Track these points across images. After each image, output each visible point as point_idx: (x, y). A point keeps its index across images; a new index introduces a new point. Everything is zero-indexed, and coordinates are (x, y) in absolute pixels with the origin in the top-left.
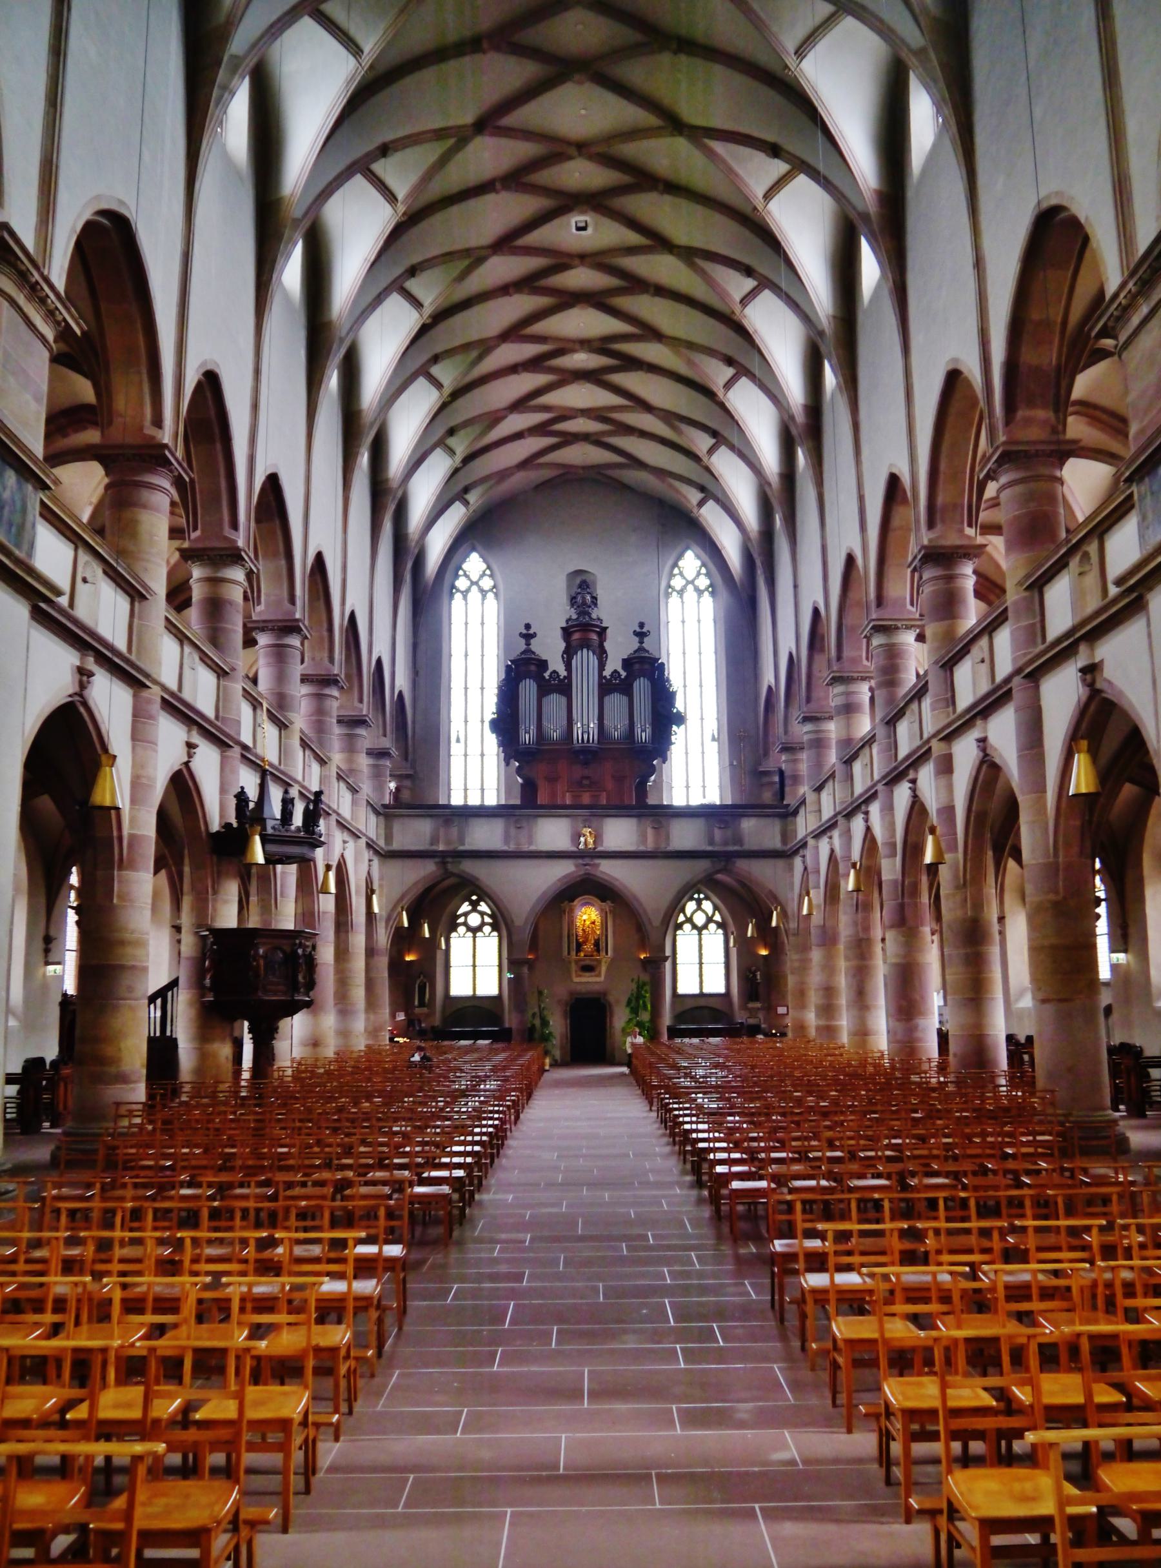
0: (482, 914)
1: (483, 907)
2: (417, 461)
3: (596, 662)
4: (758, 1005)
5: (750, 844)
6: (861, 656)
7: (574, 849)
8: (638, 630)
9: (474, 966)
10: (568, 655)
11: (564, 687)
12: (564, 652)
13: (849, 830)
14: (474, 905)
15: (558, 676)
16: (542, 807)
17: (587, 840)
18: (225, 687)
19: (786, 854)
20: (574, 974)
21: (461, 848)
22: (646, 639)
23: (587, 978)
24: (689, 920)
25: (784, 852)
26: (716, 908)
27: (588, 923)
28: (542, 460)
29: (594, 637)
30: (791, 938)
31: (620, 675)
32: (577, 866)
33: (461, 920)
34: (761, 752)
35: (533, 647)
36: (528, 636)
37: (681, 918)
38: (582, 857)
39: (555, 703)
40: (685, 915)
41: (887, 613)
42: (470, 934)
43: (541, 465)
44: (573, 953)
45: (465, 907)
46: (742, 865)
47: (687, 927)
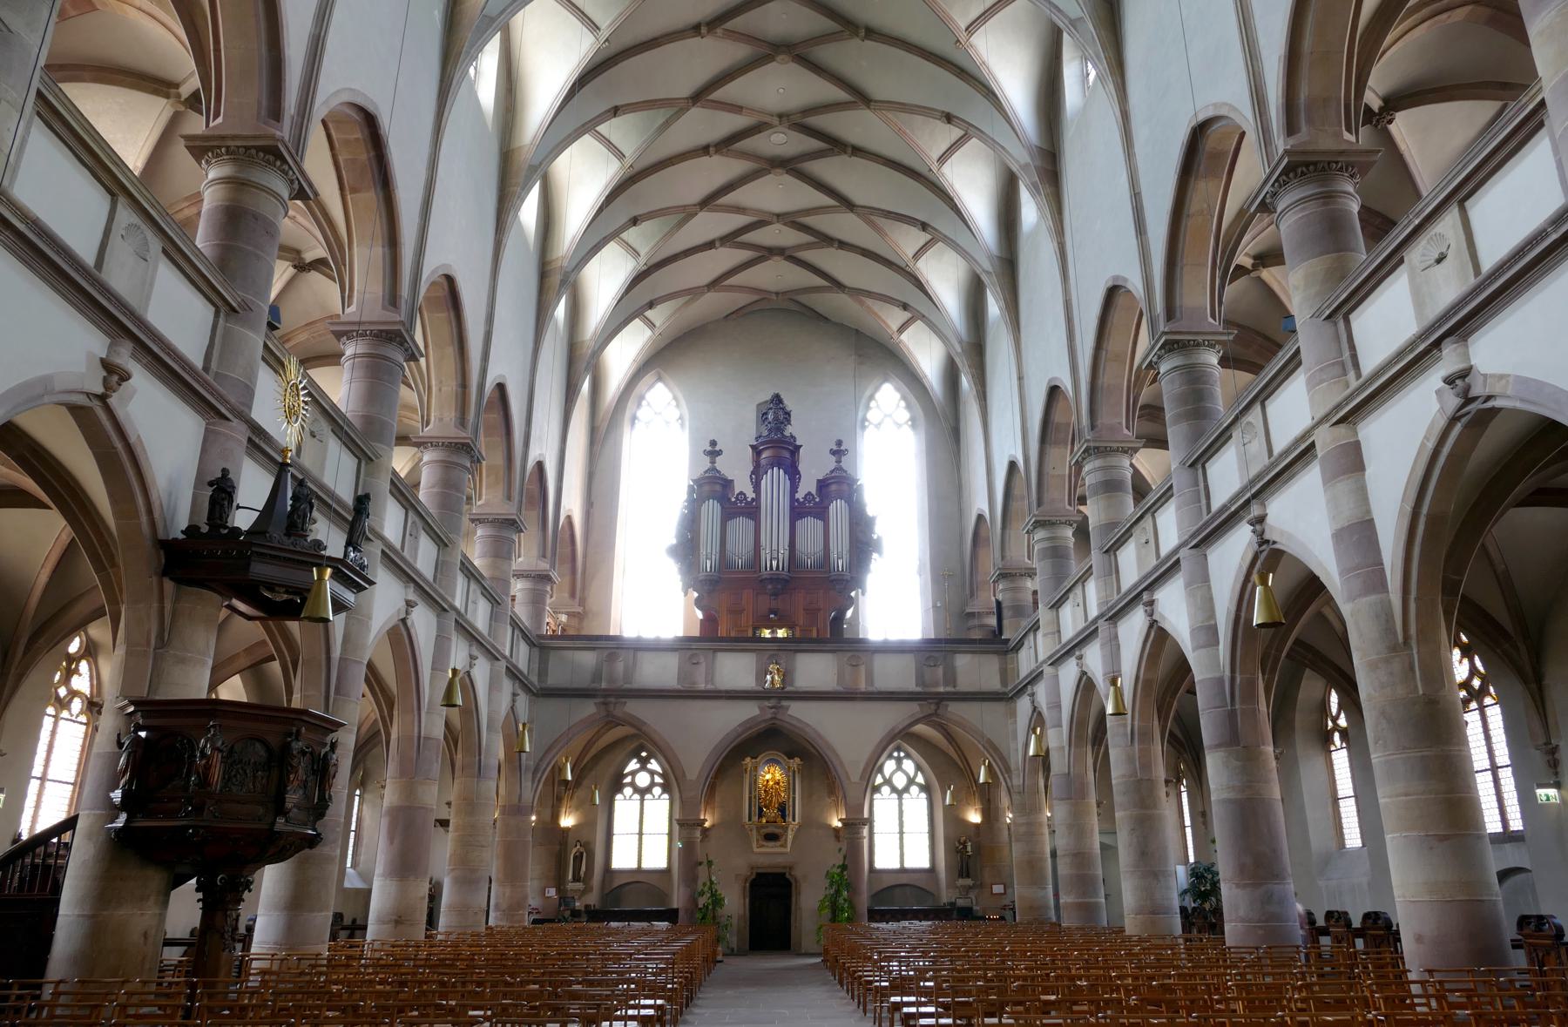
0: (652, 773)
1: (654, 765)
2: (591, 246)
3: (788, 482)
4: (969, 882)
5: (964, 684)
6: (1120, 423)
7: (761, 689)
8: (835, 448)
9: (641, 834)
10: (757, 475)
11: (751, 510)
12: (753, 473)
13: (1116, 637)
14: (644, 763)
15: (745, 498)
16: (722, 639)
17: (773, 679)
18: (227, 332)
19: (1005, 697)
20: (754, 845)
21: (627, 686)
22: (843, 459)
23: (771, 848)
24: (888, 782)
25: (1005, 693)
26: (918, 768)
27: (771, 783)
28: (732, 281)
29: (787, 455)
30: (1015, 797)
32: (761, 709)
33: (628, 780)
34: (968, 592)
35: (718, 466)
36: (714, 453)
37: (879, 780)
38: (768, 698)
39: (740, 527)
40: (883, 777)
41: (1181, 325)
42: (637, 796)
43: (732, 288)
44: (755, 818)
45: (633, 765)
46: (955, 709)
47: (886, 790)
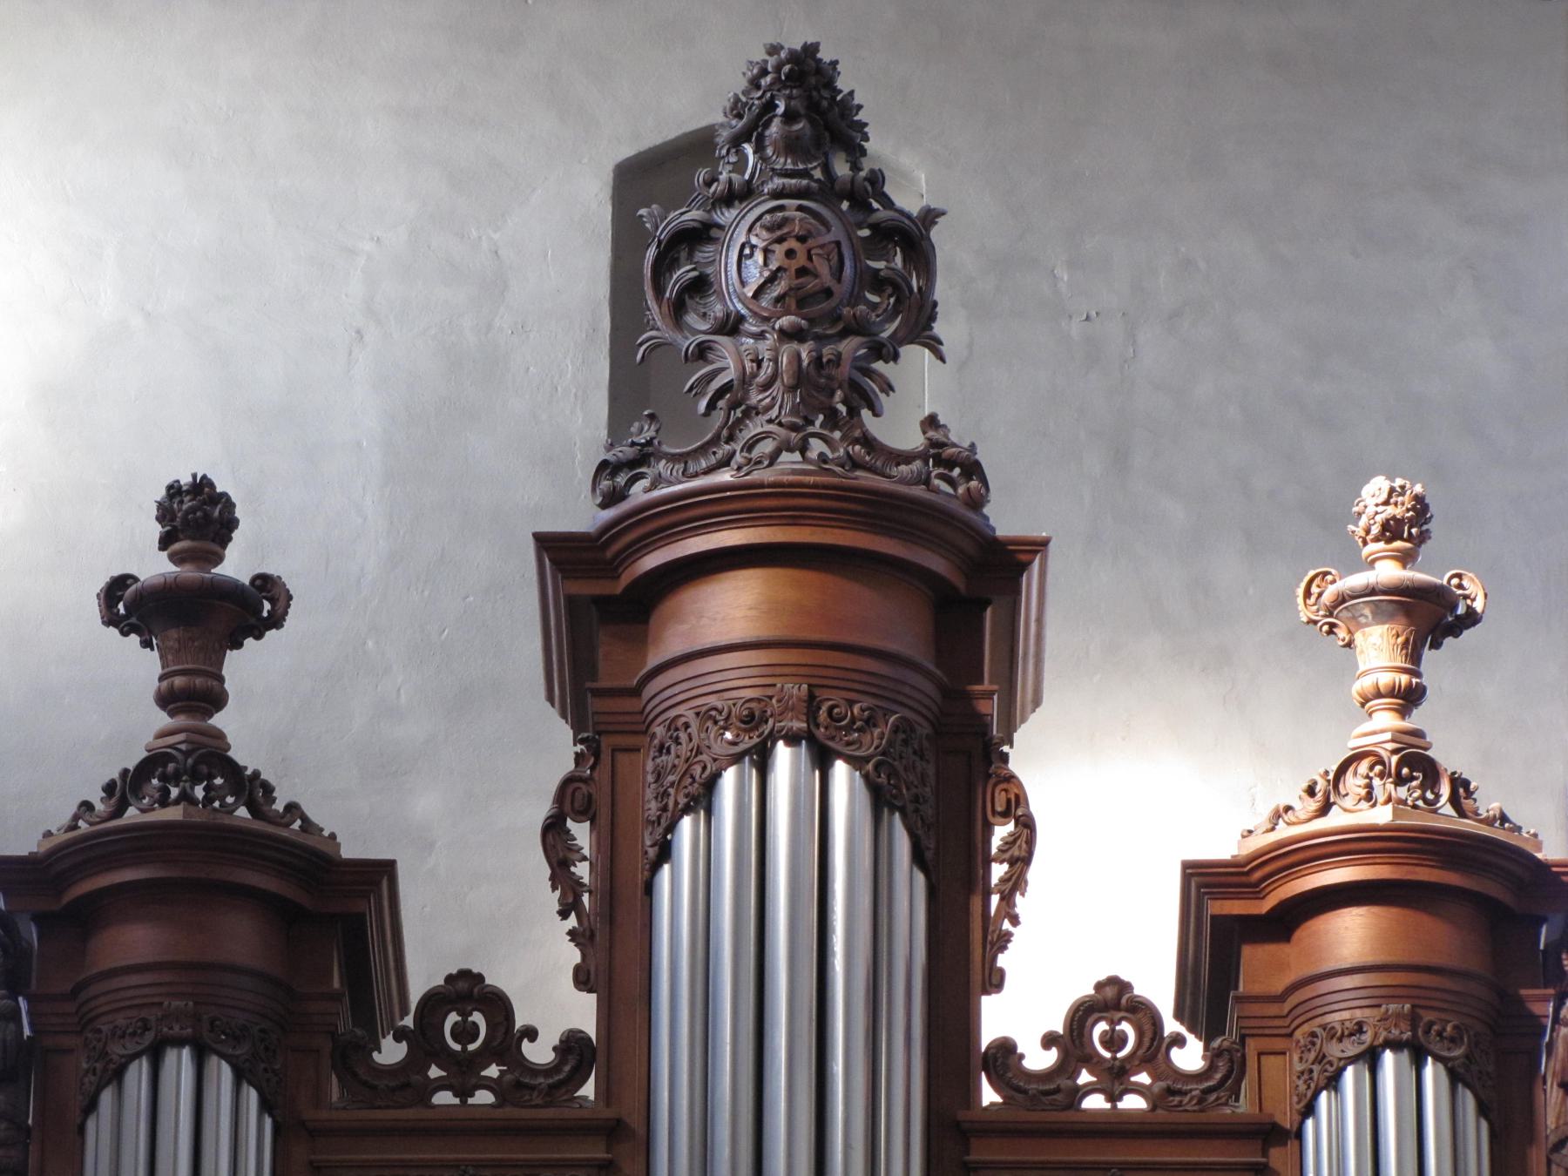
31: (1155, 1047)
